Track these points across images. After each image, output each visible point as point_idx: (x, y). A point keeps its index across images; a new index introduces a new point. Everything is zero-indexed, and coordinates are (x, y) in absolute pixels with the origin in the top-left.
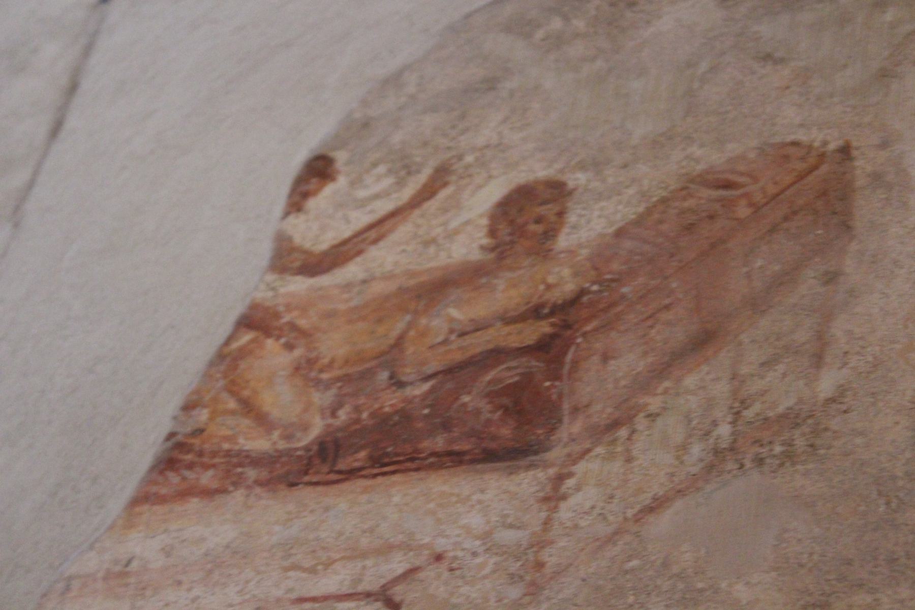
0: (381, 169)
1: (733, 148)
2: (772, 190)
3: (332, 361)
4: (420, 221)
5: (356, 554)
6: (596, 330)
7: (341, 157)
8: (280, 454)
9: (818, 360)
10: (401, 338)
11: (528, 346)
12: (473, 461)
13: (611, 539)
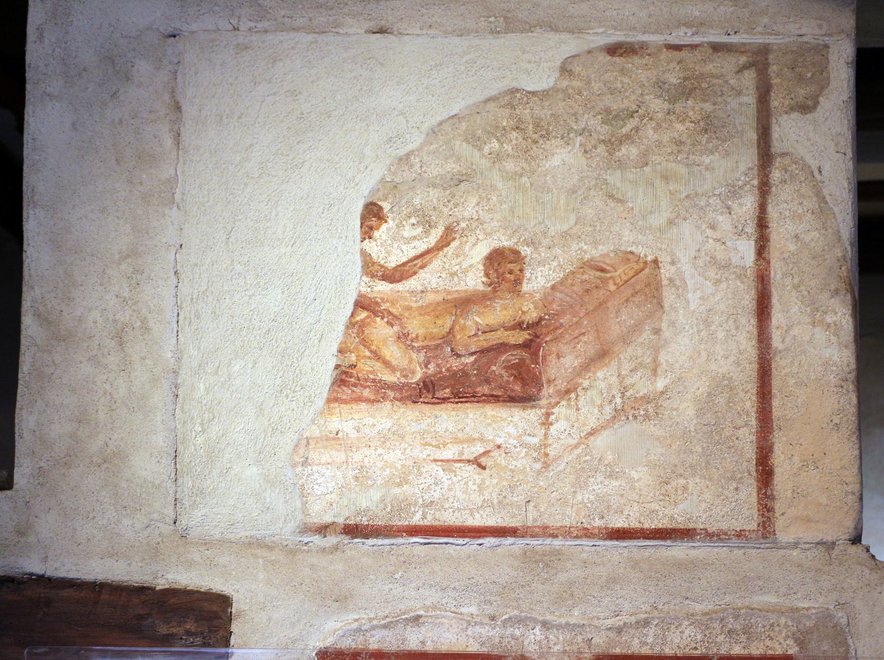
0: (413, 220)
1: (603, 249)
2: (624, 278)
3: (417, 337)
5: (457, 441)
6: (551, 341)
7: (386, 206)
8: (404, 385)
9: (655, 372)
12: (504, 401)
13: (576, 446)
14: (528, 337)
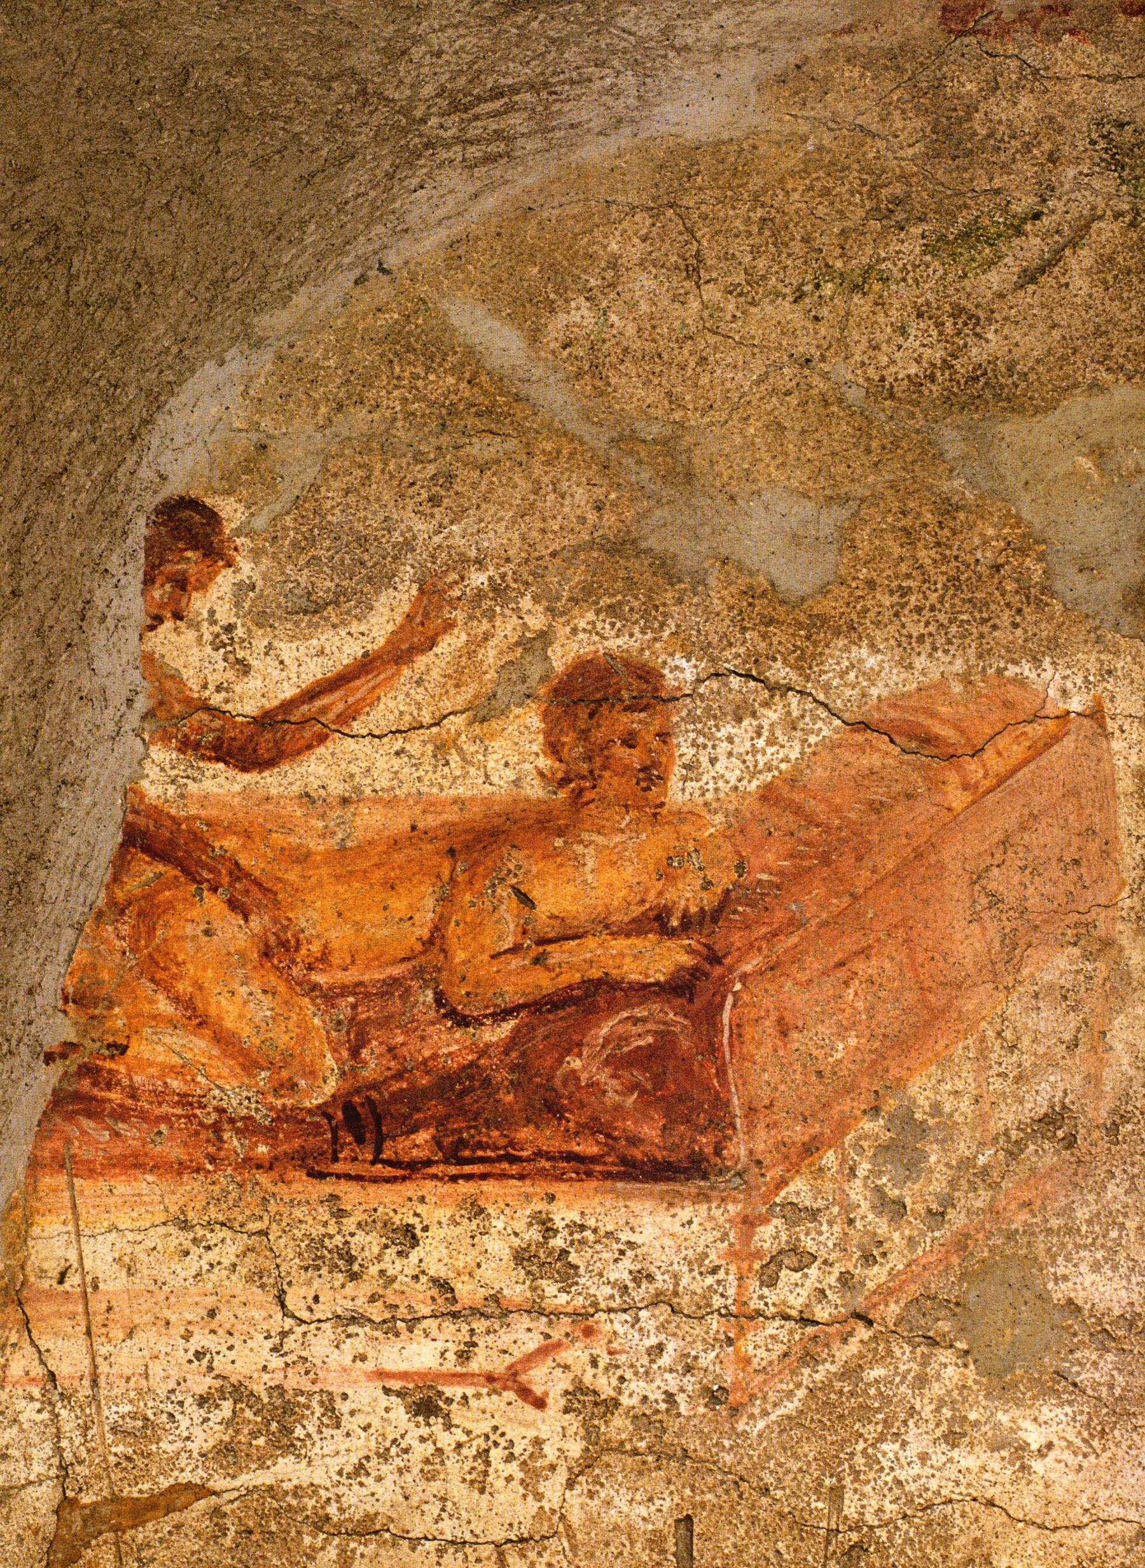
4: (419, 694)
10: (438, 929)
11: (657, 984)
12: (608, 1176)
14: (685, 959)
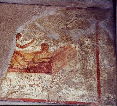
7: (22, 34)
